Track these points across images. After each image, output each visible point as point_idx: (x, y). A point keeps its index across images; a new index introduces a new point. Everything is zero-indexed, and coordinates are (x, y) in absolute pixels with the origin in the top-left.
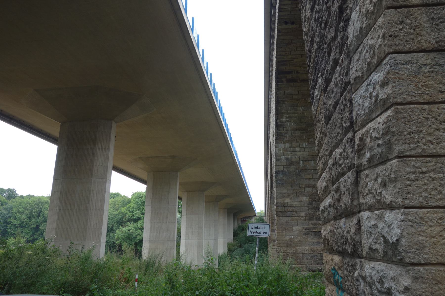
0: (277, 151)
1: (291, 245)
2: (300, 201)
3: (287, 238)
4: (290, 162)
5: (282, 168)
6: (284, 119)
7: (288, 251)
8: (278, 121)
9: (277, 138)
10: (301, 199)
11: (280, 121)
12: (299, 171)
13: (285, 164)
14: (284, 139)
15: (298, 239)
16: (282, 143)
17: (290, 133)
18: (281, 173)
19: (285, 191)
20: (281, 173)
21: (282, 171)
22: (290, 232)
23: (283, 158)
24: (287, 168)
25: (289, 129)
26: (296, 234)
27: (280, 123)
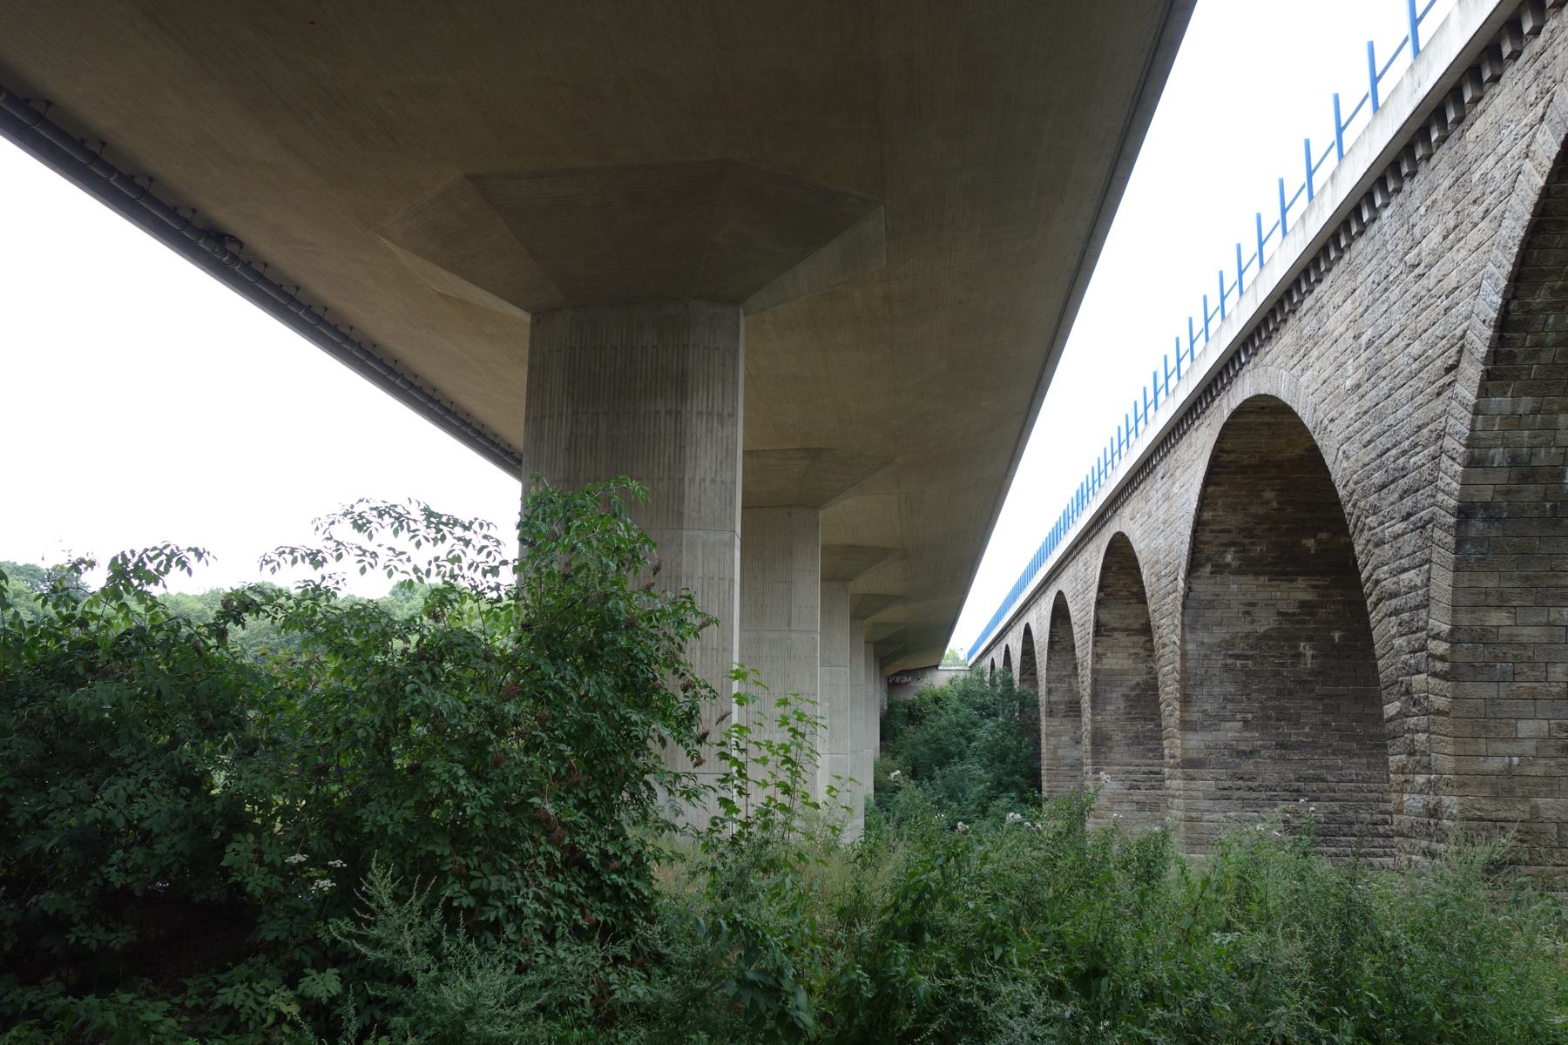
0: (1479, 426)
1: (1511, 791)
2: (1549, 624)
3: (1495, 764)
4: (1523, 470)
5: (1487, 495)
6: (1540, 298)
7: (1502, 815)
8: (1513, 305)
9: (1488, 376)
10: (1554, 615)
11: (1522, 305)
12: (1554, 508)
13: (1501, 477)
14: (1518, 378)
15: (1538, 770)
16: (1504, 394)
17: (1546, 356)
18: (1481, 514)
19: (1491, 583)
20: (1481, 514)
21: (1486, 506)
22: (1505, 739)
23: (1498, 455)
24: (1508, 492)
25: (1550, 337)
26: (1529, 747)
27: (1516, 315)
